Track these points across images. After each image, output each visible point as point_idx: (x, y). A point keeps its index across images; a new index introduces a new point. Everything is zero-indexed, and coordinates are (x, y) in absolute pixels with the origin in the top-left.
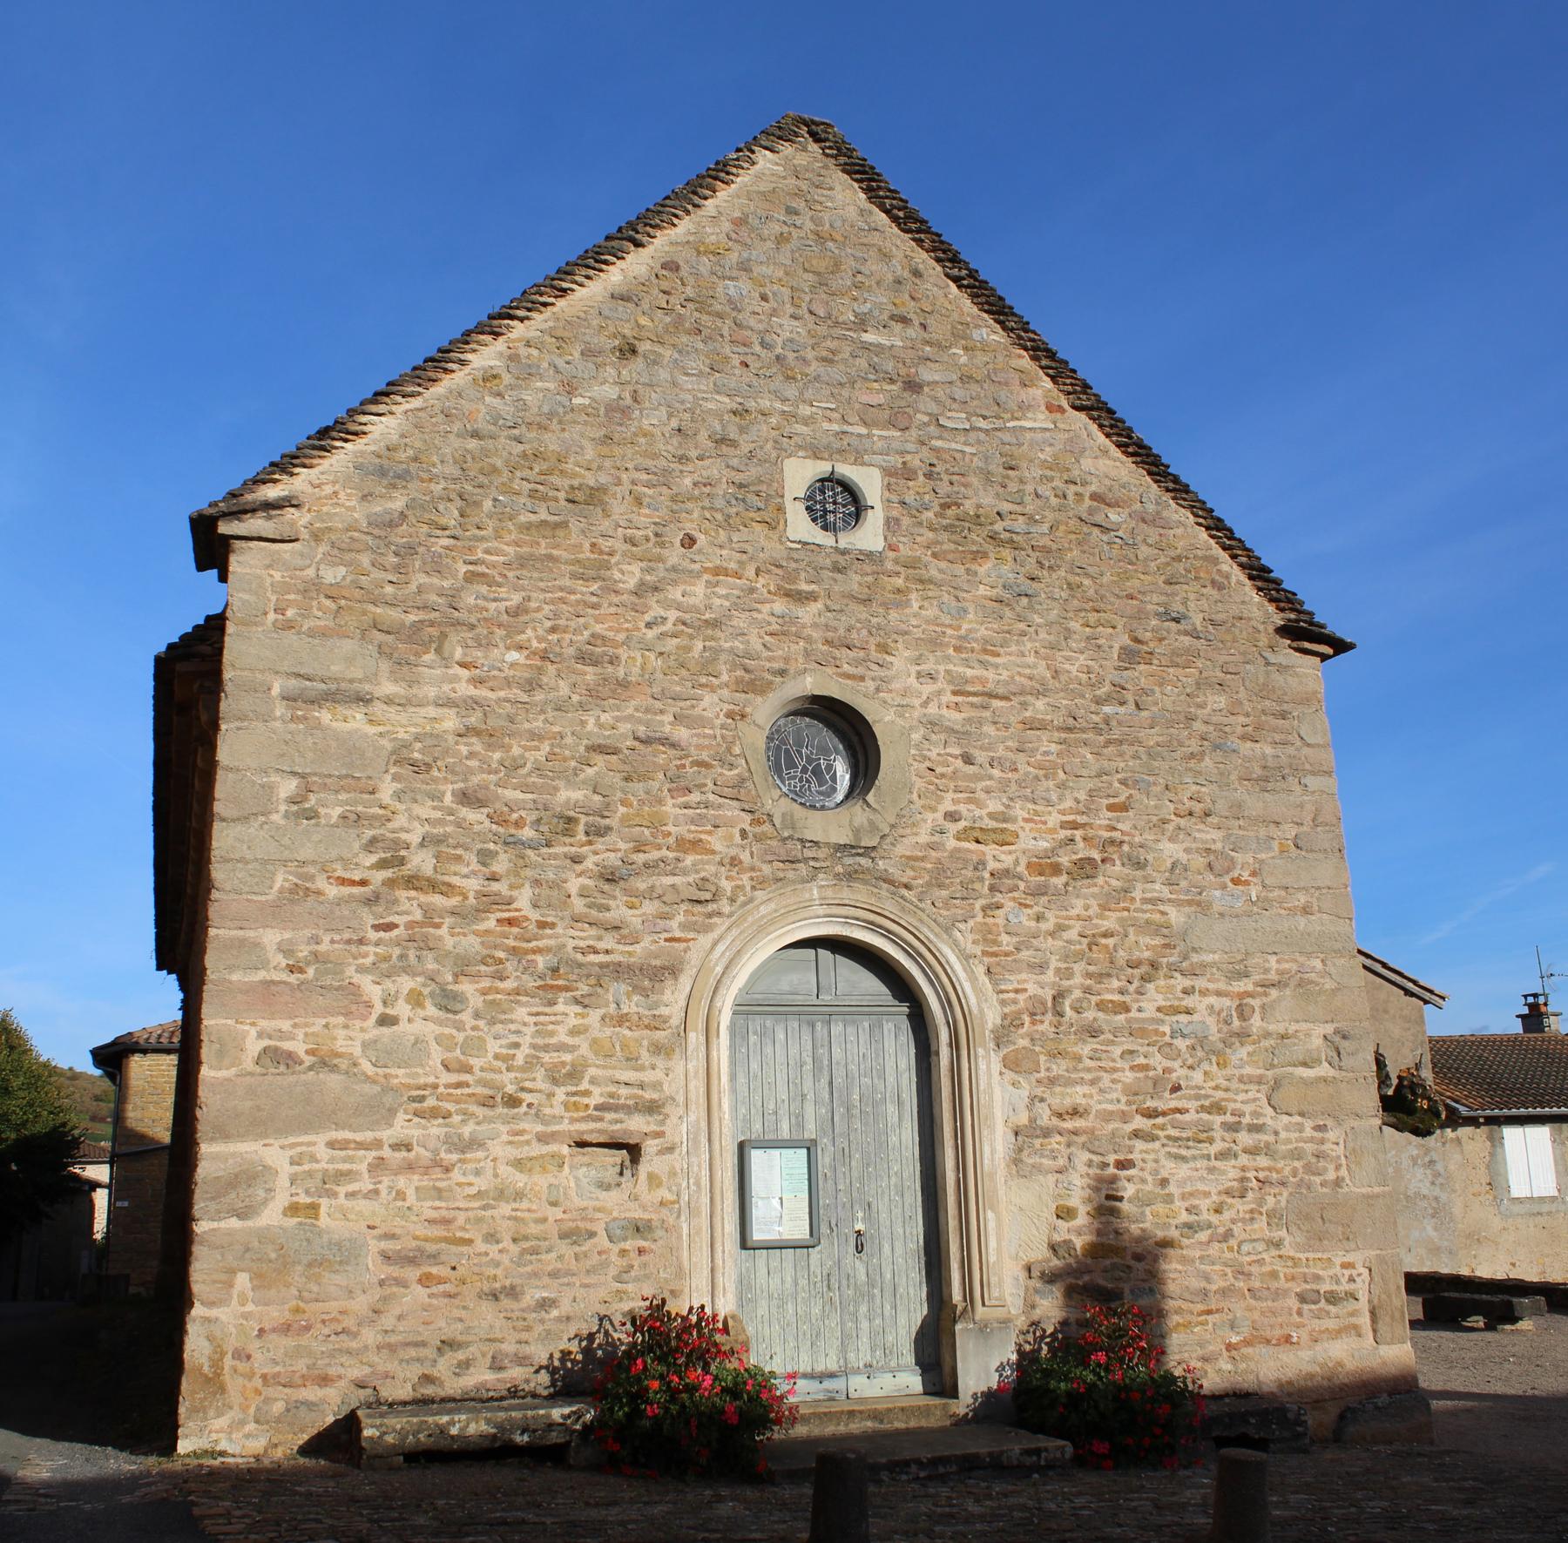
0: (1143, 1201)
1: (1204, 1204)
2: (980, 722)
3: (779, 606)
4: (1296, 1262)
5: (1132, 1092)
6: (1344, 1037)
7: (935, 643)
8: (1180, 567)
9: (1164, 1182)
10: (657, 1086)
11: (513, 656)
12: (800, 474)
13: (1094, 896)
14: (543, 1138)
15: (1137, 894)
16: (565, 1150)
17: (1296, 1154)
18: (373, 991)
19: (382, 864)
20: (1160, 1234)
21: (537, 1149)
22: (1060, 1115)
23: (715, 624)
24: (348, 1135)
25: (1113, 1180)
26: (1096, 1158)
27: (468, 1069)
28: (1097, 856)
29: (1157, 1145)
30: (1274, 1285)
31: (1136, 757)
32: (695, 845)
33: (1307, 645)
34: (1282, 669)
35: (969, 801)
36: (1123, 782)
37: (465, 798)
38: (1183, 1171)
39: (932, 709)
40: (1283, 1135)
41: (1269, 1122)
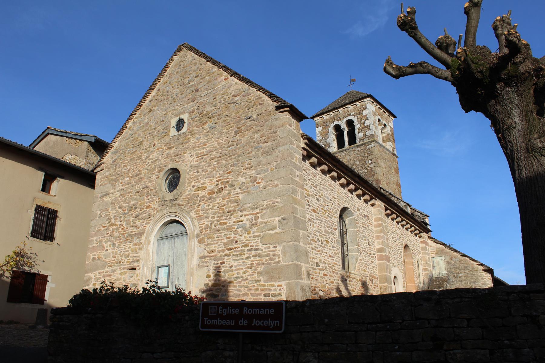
0: (226, 272)
1: (241, 271)
2: (201, 162)
3: (168, 152)
4: (264, 286)
5: (225, 244)
6: (284, 220)
7: (194, 148)
8: (251, 104)
9: (231, 267)
10: (139, 256)
11: (128, 179)
12: (174, 122)
13: (221, 197)
14: (124, 269)
15: (232, 194)
16: (126, 270)
17: (268, 255)
18: (105, 245)
19: (109, 223)
20: (229, 280)
21: (123, 271)
22: (208, 252)
23: (156, 160)
24: (100, 271)
25: (219, 267)
26: (216, 262)
27: (115, 257)
28: (223, 186)
29: (230, 257)
30: (257, 292)
31: (235, 158)
32: (149, 207)
33: (281, 110)
34: (277, 119)
35: (198, 182)
36: (231, 166)
37: (120, 208)
38: (236, 263)
39: (192, 163)
40: (264, 250)
41: (260, 247)
